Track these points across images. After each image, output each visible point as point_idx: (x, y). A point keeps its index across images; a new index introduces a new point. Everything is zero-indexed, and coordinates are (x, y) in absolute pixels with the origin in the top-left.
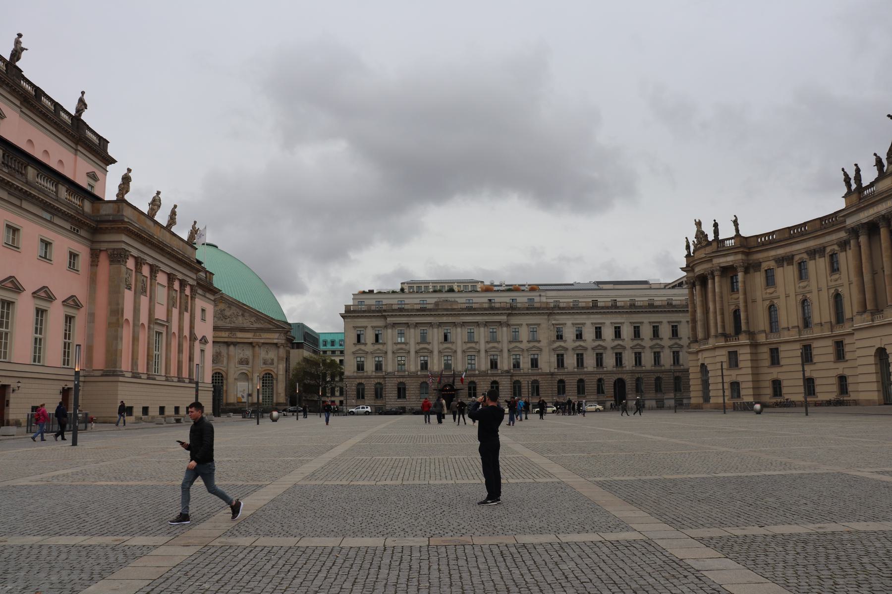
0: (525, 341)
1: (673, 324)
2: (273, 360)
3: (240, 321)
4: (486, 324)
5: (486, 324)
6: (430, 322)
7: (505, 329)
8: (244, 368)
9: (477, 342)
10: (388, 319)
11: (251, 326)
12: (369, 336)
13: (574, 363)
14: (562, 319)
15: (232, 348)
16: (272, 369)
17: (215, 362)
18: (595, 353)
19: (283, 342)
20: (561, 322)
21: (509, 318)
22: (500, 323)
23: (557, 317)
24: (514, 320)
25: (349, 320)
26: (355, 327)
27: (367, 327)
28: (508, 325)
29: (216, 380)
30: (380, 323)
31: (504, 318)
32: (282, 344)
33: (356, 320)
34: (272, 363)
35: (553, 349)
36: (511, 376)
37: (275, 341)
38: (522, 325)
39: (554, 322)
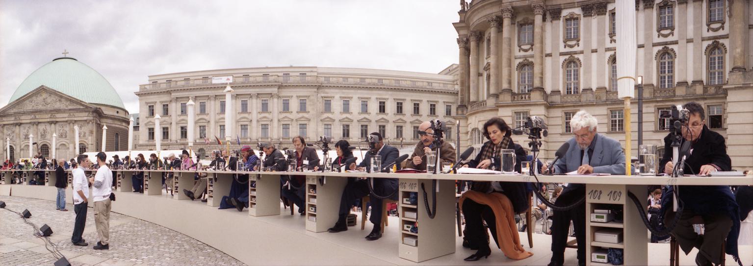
0: (294, 112)
1: (399, 101)
2: (85, 133)
3: (58, 105)
4: (258, 95)
5: (258, 95)
6: (208, 95)
7: (276, 100)
8: (63, 141)
9: (250, 113)
10: (173, 94)
11: (67, 108)
12: (159, 110)
13: (340, 134)
14: (330, 92)
15: (53, 125)
16: (85, 140)
17: (43, 137)
18: (360, 125)
19: (92, 118)
20: (329, 95)
21: (280, 90)
22: (271, 95)
23: (327, 90)
24: (285, 93)
25: (143, 98)
26: (147, 103)
27: (156, 102)
28: (279, 97)
29: (46, 150)
30: (165, 98)
31: (275, 90)
32: (90, 120)
33: (148, 97)
34: (84, 136)
35: (321, 120)
36: (280, 144)
37: (85, 118)
38: (292, 97)
39: (323, 95)
